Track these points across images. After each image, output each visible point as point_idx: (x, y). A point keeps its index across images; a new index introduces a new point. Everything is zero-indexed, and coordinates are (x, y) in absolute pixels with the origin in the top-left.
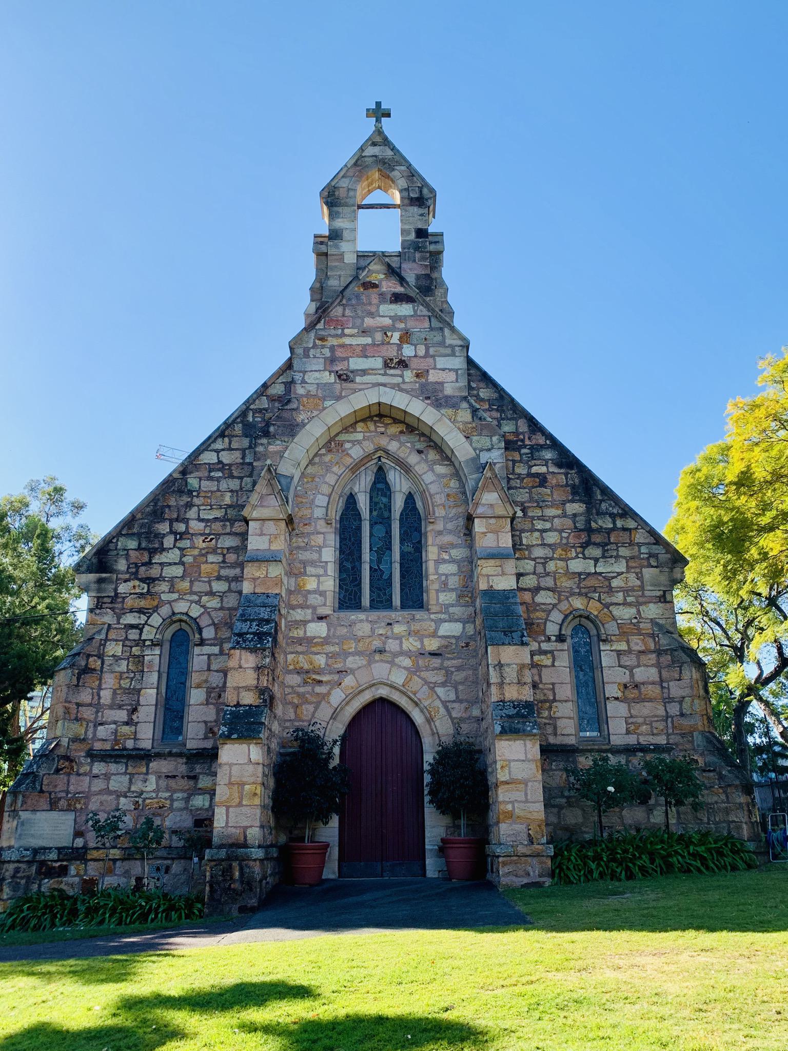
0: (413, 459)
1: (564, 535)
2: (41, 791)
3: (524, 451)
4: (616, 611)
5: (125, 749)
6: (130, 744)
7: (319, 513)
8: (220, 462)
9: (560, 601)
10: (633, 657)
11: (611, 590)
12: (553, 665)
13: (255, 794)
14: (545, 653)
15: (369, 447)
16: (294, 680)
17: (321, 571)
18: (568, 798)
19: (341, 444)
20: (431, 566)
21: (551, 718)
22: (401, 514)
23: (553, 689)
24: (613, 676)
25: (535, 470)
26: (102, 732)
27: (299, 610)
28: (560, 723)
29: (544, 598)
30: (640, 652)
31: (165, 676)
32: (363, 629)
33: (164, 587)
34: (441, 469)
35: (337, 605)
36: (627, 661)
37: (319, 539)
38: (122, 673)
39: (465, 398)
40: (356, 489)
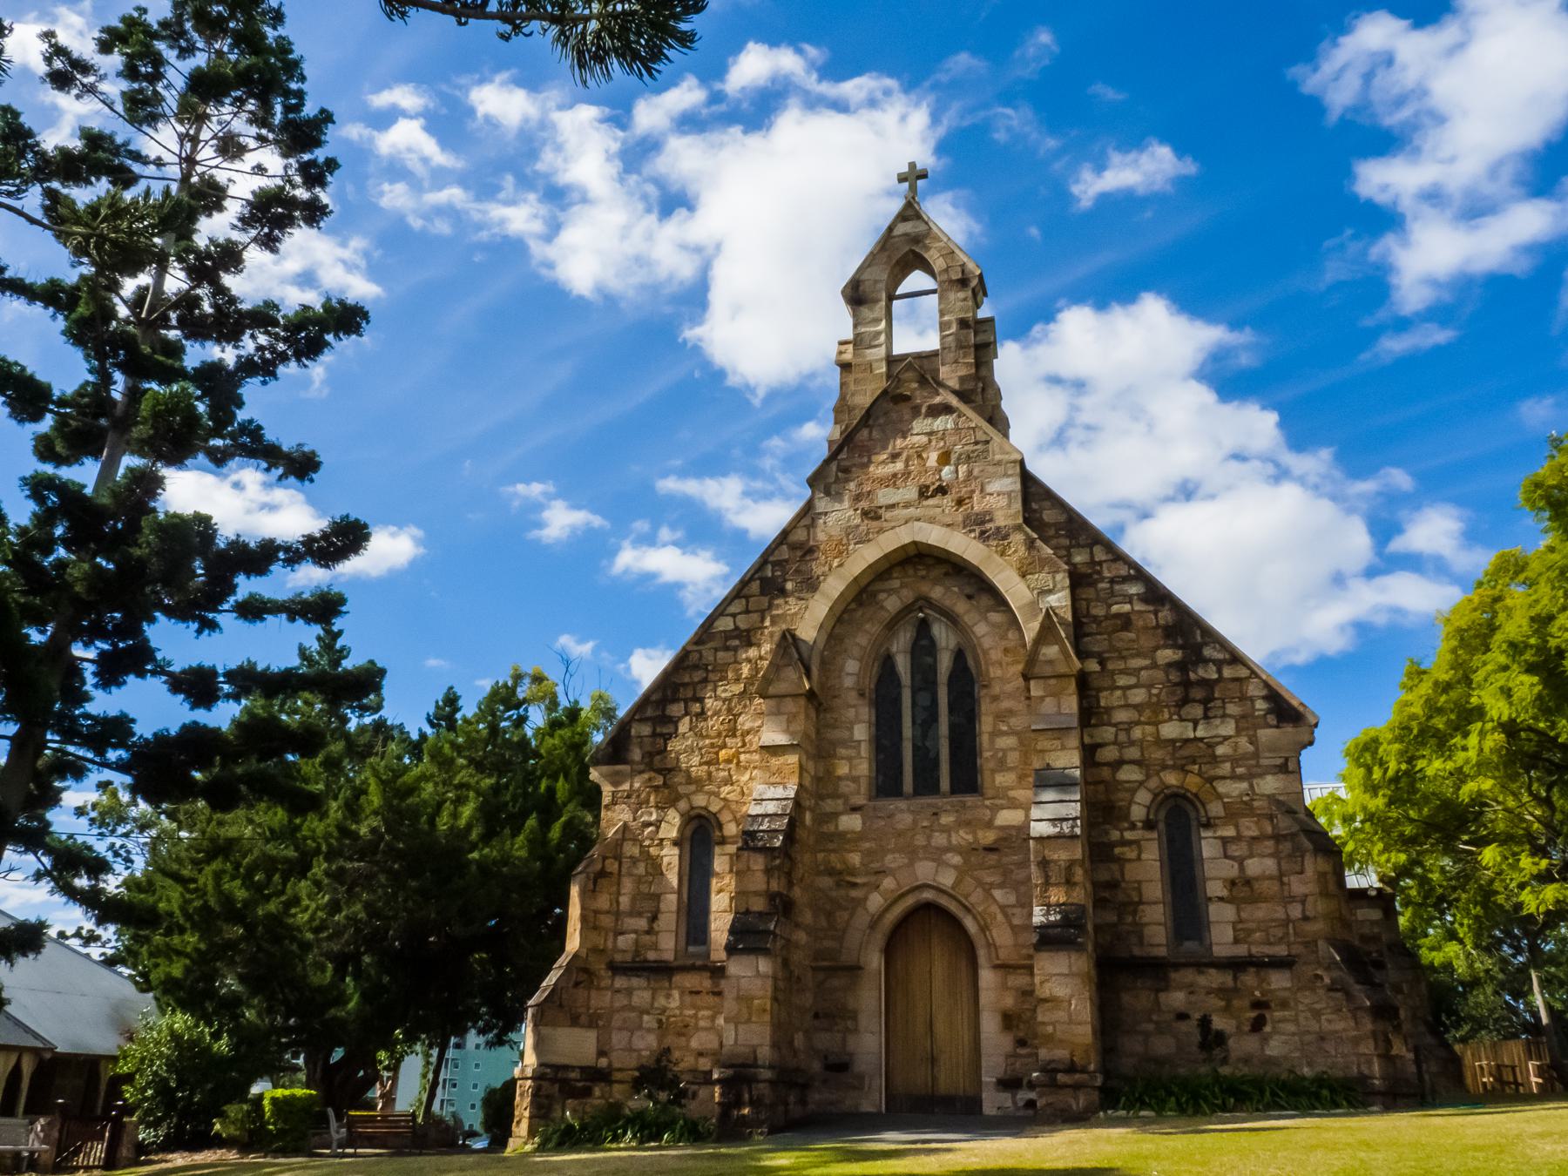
0: (961, 607)
1: (1155, 691)
2: (561, 1006)
3: (1102, 585)
4: (1222, 787)
5: (646, 961)
6: (651, 956)
7: (849, 682)
8: (737, 628)
9: (1148, 777)
10: (1244, 845)
11: (1215, 760)
12: (1139, 858)
13: (765, 1010)
14: (1129, 843)
15: (908, 595)
16: (826, 882)
18: (1157, 1023)
19: (874, 595)
20: (985, 739)
21: (1135, 923)
22: (950, 677)
23: (1139, 890)
24: (1216, 869)
25: (1115, 608)
26: (625, 941)
27: (829, 801)
28: (1147, 931)
29: (1129, 774)
30: (1253, 838)
31: (686, 879)
32: (905, 820)
33: (679, 779)
34: (996, 617)
36: (1235, 850)
37: (851, 713)
38: (640, 877)
39: (1018, 528)
40: (894, 649)
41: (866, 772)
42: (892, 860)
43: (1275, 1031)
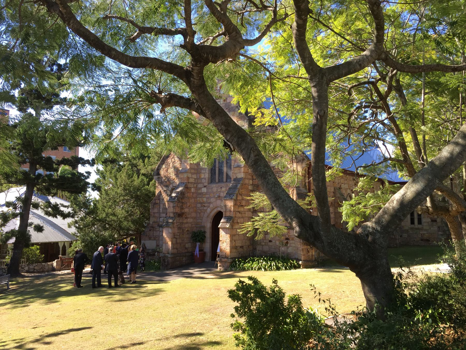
2: (146, 236)
16: (199, 205)
17: (205, 172)
32: (215, 190)
35: (210, 182)
41: (207, 177)
42: (212, 200)
43: (290, 246)
